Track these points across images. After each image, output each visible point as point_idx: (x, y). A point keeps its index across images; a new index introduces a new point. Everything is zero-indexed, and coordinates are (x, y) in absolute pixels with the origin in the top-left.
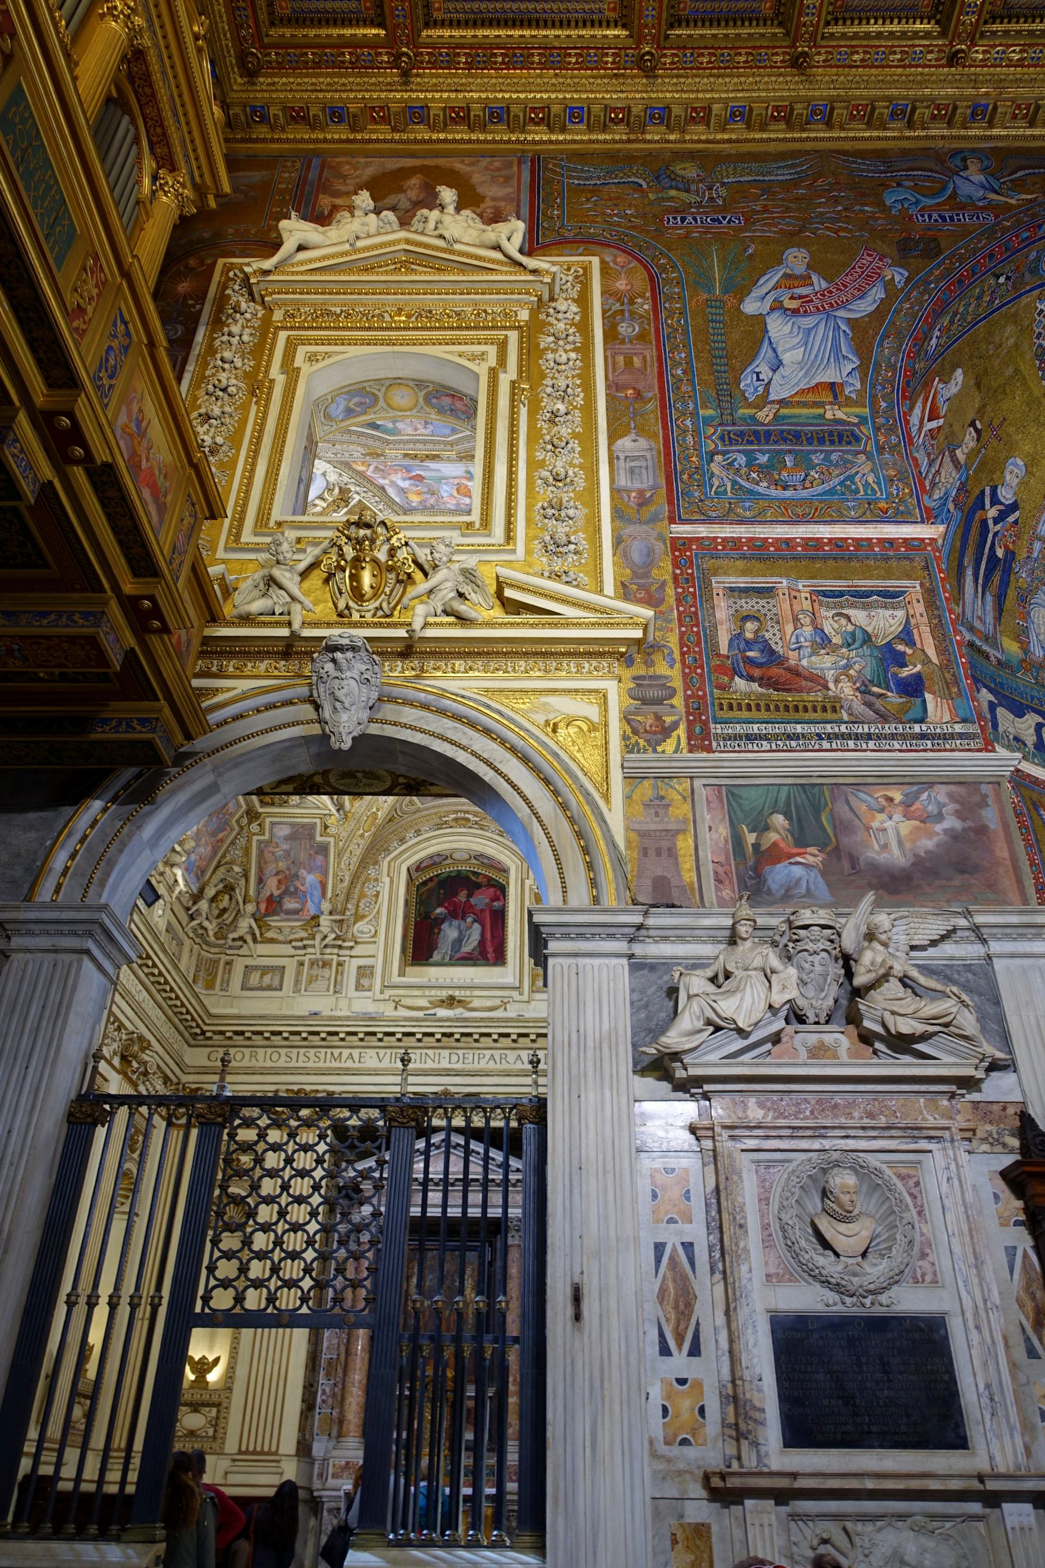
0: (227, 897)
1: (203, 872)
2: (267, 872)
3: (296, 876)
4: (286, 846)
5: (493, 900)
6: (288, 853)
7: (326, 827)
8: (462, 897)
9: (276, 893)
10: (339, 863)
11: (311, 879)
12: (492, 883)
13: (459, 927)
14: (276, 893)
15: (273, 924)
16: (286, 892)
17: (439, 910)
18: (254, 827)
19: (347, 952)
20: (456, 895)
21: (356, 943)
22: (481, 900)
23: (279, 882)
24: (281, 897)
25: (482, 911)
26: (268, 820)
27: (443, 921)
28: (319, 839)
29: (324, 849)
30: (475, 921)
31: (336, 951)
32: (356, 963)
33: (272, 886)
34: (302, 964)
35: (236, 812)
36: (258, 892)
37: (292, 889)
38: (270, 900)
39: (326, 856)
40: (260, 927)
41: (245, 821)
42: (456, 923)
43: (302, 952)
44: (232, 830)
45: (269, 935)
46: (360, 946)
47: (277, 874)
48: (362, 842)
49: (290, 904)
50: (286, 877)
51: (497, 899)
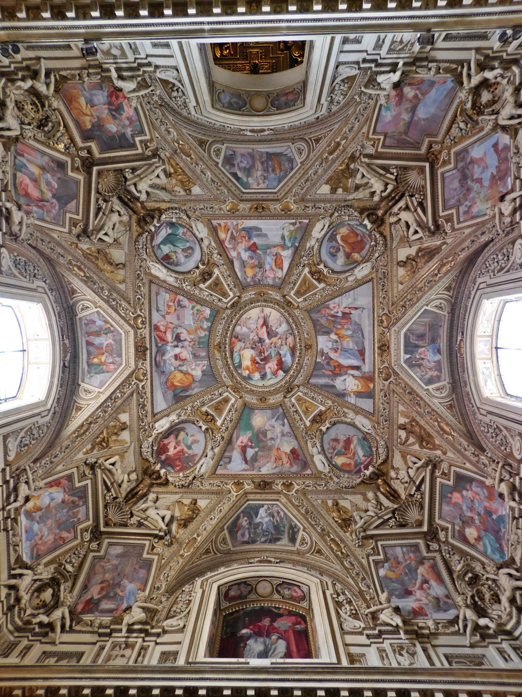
0: (50, 591)
1: (39, 557)
2: (93, 581)
3: (119, 585)
4: (115, 562)
5: (295, 624)
6: (116, 567)
7: (153, 548)
8: (266, 622)
9: (96, 597)
10: (159, 575)
11: (130, 587)
12: (291, 613)
13: (264, 643)
14: (96, 597)
15: (84, 618)
16: (106, 597)
17: (244, 631)
18: (94, 545)
19: (154, 638)
20: (260, 621)
21: (165, 632)
22: (283, 624)
23: (102, 589)
24: (99, 600)
25: (285, 631)
26: (106, 541)
27: (249, 637)
28: (145, 556)
29: (148, 564)
30: (279, 638)
31: (143, 635)
32: (160, 649)
33: (94, 592)
34: (102, 648)
35: (83, 522)
36: (80, 596)
37: (112, 594)
38: (89, 602)
39: (149, 571)
40: (71, 621)
41: (87, 536)
42: (260, 640)
43: (107, 638)
44: (76, 538)
45: (78, 628)
46: (167, 636)
47: (102, 583)
48: (181, 560)
49: (106, 605)
50: (109, 585)
51: (300, 623)
